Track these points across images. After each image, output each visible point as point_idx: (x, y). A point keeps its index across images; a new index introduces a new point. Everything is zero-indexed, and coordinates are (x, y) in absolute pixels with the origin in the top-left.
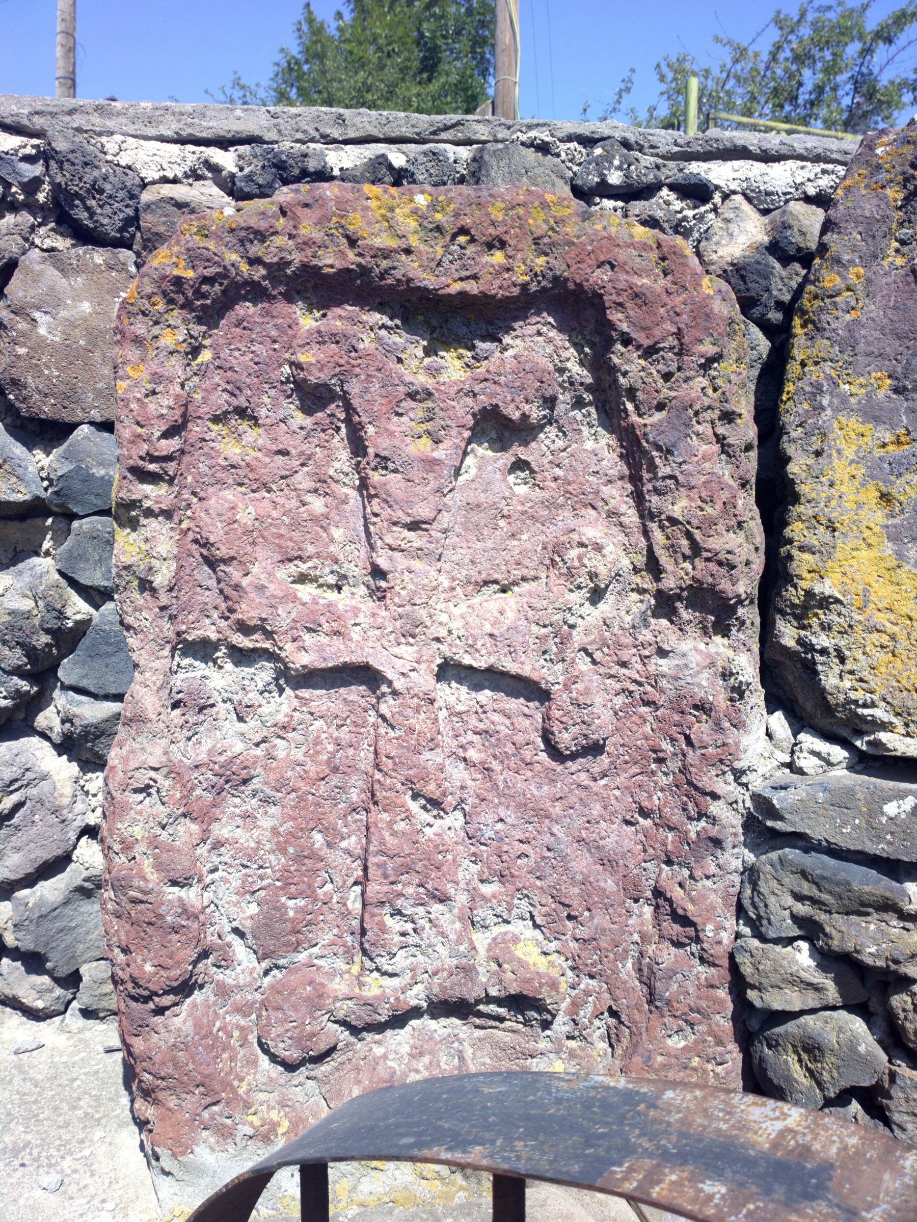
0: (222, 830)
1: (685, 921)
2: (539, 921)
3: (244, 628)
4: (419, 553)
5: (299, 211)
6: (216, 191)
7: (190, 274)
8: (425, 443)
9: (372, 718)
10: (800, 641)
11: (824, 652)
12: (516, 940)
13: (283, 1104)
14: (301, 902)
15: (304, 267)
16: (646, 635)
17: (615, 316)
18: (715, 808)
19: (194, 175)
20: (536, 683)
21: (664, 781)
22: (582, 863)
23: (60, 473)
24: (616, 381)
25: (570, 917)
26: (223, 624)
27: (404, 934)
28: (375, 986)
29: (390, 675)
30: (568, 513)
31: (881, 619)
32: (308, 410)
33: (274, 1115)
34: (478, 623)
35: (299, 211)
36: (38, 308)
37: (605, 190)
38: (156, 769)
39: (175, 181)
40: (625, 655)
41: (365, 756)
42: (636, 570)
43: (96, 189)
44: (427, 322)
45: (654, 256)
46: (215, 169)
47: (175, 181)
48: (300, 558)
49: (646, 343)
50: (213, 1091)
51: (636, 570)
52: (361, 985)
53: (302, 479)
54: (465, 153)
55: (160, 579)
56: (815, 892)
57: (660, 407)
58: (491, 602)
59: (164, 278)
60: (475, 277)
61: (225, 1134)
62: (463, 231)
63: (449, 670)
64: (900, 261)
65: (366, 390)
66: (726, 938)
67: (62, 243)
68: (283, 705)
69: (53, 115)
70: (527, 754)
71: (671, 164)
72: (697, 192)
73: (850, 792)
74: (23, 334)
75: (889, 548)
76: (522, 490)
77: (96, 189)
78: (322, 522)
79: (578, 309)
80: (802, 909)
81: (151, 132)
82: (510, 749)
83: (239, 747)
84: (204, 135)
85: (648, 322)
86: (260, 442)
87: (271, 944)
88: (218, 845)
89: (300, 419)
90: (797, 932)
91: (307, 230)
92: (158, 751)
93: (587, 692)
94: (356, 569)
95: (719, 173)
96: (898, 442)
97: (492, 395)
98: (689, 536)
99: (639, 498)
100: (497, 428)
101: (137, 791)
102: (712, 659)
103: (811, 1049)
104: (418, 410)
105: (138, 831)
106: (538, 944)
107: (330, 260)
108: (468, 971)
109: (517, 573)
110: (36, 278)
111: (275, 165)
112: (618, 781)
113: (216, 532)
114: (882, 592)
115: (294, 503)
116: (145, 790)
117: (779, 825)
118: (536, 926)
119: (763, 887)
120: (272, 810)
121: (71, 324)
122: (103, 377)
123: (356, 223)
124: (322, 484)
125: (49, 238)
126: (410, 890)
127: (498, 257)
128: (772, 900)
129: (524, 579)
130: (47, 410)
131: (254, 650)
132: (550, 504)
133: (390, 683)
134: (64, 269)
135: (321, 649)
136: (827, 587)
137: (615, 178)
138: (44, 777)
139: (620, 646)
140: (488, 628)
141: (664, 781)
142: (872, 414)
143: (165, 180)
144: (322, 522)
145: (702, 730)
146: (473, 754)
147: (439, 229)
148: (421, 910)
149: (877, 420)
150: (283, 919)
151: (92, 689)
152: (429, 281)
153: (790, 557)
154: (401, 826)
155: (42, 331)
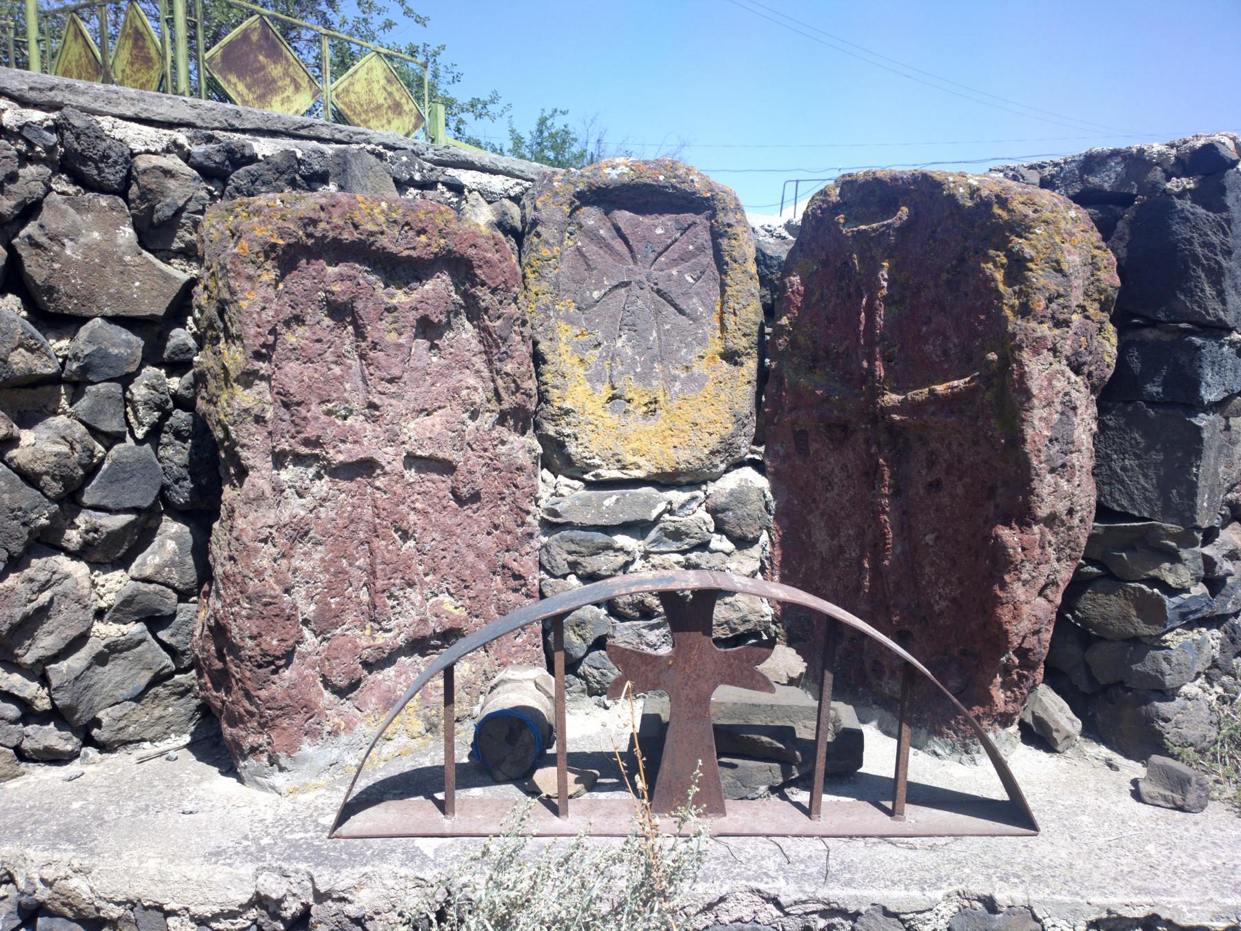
0: (296, 563)
1: (517, 577)
2: (452, 591)
3: (307, 442)
4: (393, 396)
5: (331, 209)
6: (179, 161)
7: (281, 242)
8: (394, 335)
9: (369, 490)
10: (557, 432)
11: (568, 436)
12: (442, 603)
13: (339, 715)
14: (337, 599)
15: (334, 239)
16: (495, 434)
17: (478, 272)
18: (529, 519)
19: (167, 151)
20: (450, 462)
21: (504, 509)
22: (471, 558)
23: (86, 353)
24: (478, 303)
25: (466, 587)
26: (292, 441)
27: (393, 607)
28: (381, 638)
29: (384, 463)
30: (457, 372)
31: (591, 418)
32: (331, 315)
33: (337, 720)
34: (422, 432)
35: (331, 209)
36: (67, 237)
37: (412, 183)
38: (271, 527)
39: (155, 153)
40: (487, 444)
41: (368, 512)
42: (489, 401)
43: (105, 157)
44: (384, 268)
45: (492, 242)
46: (181, 147)
47: (155, 153)
48: (328, 401)
49: (493, 286)
50: (308, 709)
51: (489, 401)
52: (374, 639)
53: (329, 356)
54: (329, 149)
55: (269, 415)
56: (578, 549)
57: (499, 318)
58: (428, 421)
59: (266, 243)
60: (414, 248)
61: (313, 734)
62: (407, 224)
63: (412, 460)
64: (571, 243)
65: (366, 307)
66: (536, 582)
67: (71, 189)
68: (323, 486)
69: (41, 90)
70: (445, 502)
71: (439, 168)
72: (457, 188)
73: (589, 499)
74: (57, 254)
75: (588, 385)
76: (435, 359)
77: (105, 157)
78: (340, 379)
79: (459, 266)
80: (571, 558)
81: (116, 111)
82: (436, 500)
83: (302, 513)
84: (157, 118)
85: (493, 275)
86: (307, 335)
87: (324, 625)
88: (295, 570)
89: (328, 322)
90: (568, 571)
91: (337, 220)
92: (273, 516)
93: (473, 465)
94: (357, 403)
95: (466, 177)
96: (582, 334)
97: (426, 310)
98: (514, 381)
99: (490, 362)
100: (428, 329)
101: (261, 541)
102: (522, 447)
103: (580, 624)
104: (389, 318)
105: (265, 563)
106: (452, 604)
107: (347, 236)
108: (424, 621)
109: (436, 405)
110: (64, 214)
111: (227, 151)
112: (484, 512)
113: (293, 387)
114: (589, 406)
115: (325, 369)
116: (265, 541)
117: (559, 520)
118: (451, 595)
119: (553, 552)
120: (320, 548)
121: (89, 247)
122: (114, 285)
123: (358, 218)
124: (340, 359)
125: (62, 184)
126: (398, 581)
127: (423, 238)
128: (558, 557)
129: (440, 408)
130: (70, 307)
131: (306, 456)
132: (448, 367)
133: (383, 468)
134: (79, 208)
135: (349, 451)
136: (567, 405)
137: (417, 177)
138: (67, 577)
139: (484, 440)
140: (428, 435)
141: (504, 509)
142: (570, 321)
143: (148, 152)
144: (340, 379)
145: (521, 480)
146: (418, 505)
147: (395, 222)
148: (401, 593)
149: (572, 323)
150: (330, 610)
151: (111, 506)
152: (393, 249)
153: (547, 391)
154: (391, 547)
155: (68, 252)
